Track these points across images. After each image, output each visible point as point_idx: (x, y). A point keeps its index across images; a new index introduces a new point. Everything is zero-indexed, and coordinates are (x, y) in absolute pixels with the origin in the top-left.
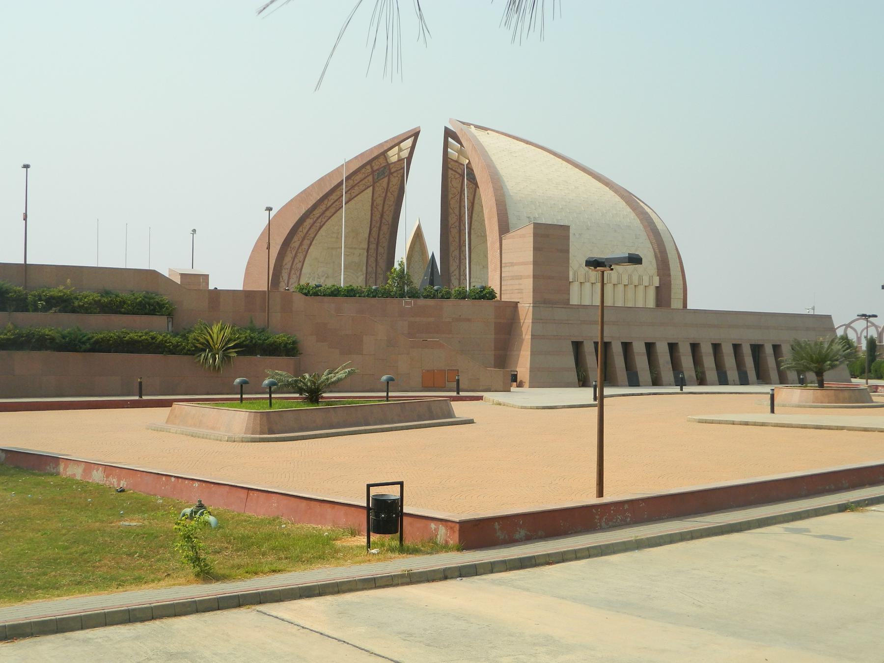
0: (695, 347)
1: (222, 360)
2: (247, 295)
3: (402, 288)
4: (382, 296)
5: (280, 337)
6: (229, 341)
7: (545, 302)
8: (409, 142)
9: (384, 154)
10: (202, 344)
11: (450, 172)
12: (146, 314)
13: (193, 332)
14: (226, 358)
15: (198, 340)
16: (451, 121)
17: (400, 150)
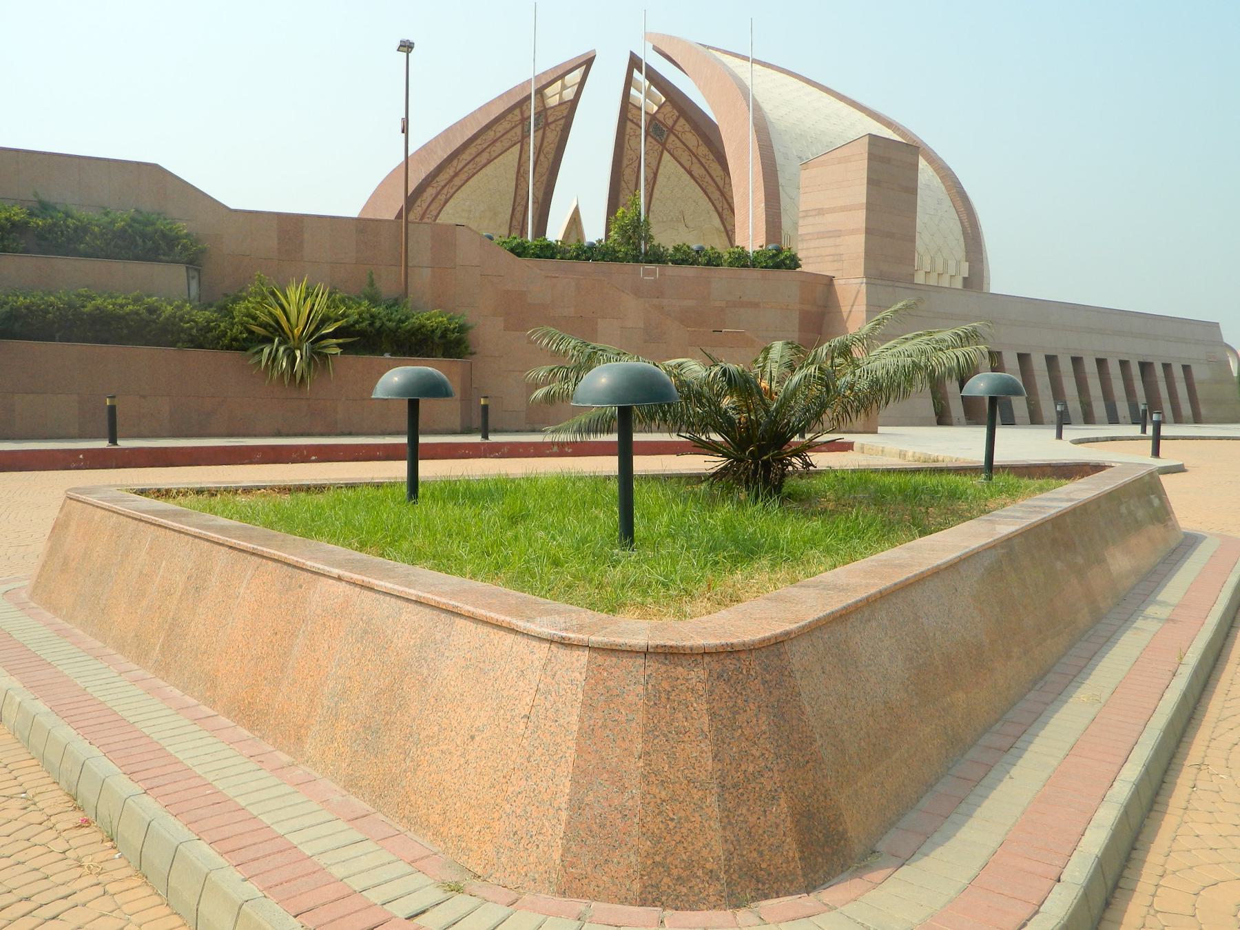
0: (1077, 361)
1: (310, 361)
2: (362, 226)
3: (638, 247)
4: (603, 259)
5: (431, 317)
6: (324, 321)
7: (882, 276)
8: (576, 75)
9: (540, 92)
10: (264, 326)
11: (629, 123)
12: (137, 258)
13: (244, 299)
14: (318, 358)
15: (255, 318)
16: (648, 36)
17: (564, 87)
